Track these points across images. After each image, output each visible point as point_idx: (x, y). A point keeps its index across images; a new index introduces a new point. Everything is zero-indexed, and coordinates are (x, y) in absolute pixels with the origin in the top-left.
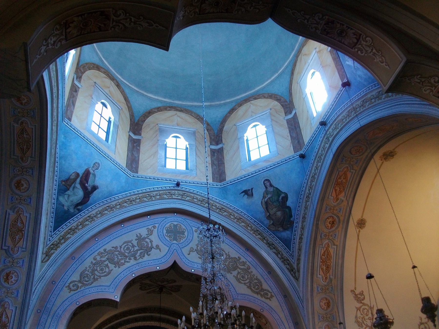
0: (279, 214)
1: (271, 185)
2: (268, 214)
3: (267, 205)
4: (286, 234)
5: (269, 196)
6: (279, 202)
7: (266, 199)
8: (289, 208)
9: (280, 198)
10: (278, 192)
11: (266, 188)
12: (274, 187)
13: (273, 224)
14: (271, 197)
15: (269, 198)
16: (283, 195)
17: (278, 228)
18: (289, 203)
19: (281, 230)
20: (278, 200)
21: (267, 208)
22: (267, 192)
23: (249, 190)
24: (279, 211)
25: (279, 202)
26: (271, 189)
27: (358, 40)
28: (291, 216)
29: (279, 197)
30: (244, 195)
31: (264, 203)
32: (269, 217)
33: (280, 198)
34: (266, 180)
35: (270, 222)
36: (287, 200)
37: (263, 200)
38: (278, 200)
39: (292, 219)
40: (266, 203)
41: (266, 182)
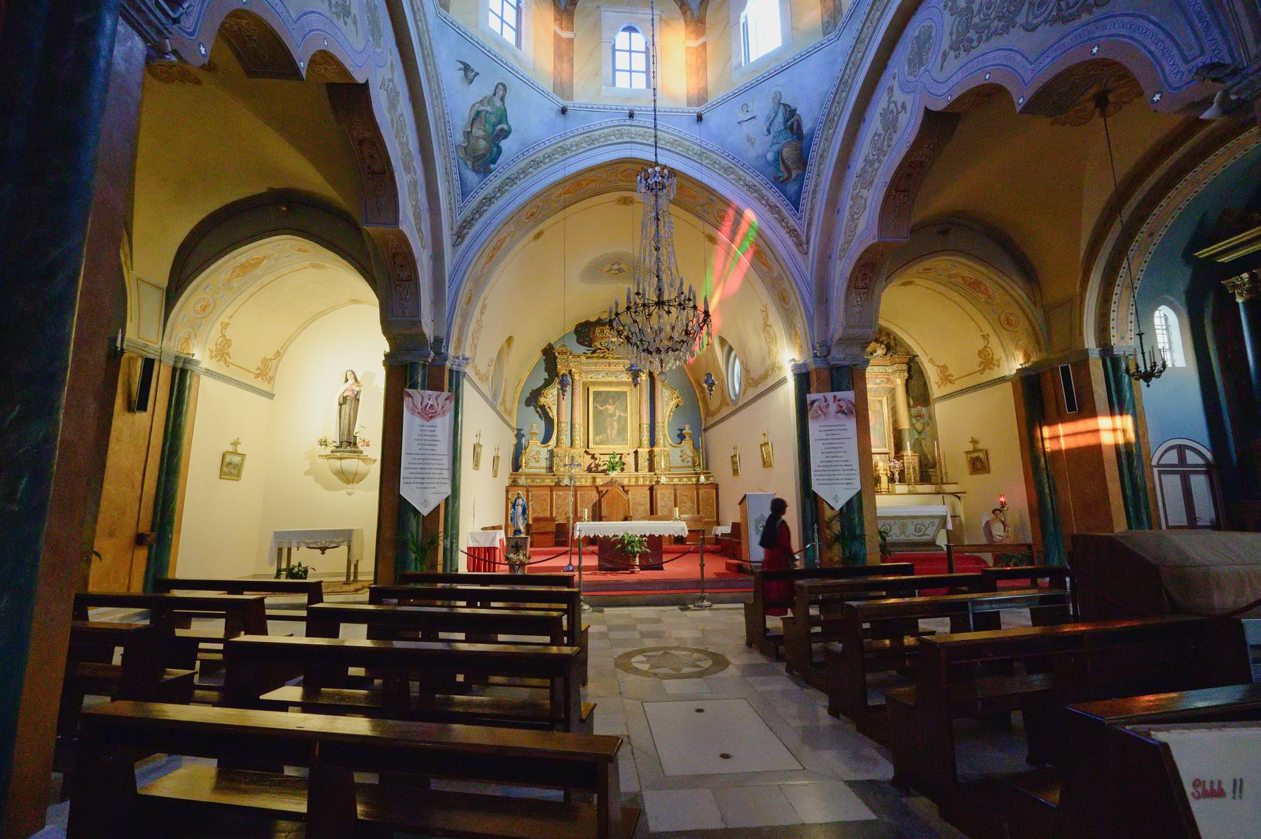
0: (482, 143)
1: (502, 99)
2: (469, 130)
3: (477, 116)
4: (471, 177)
5: (489, 109)
6: (494, 130)
7: (481, 108)
8: (500, 151)
9: (499, 127)
10: (503, 117)
11: (495, 94)
12: (503, 105)
13: (465, 148)
14: (490, 113)
15: (487, 112)
16: (505, 127)
17: (468, 160)
18: (504, 144)
19: (470, 167)
20: (494, 126)
21: (474, 119)
22: (489, 101)
23: (473, 70)
24: (485, 139)
25: (494, 130)
26: (498, 104)
27: (904, 191)
28: (494, 161)
29: (499, 124)
30: (461, 69)
31: (476, 109)
32: (468, 135)
33: (499, 127)
34: (504, 85)
35: (464, 142)
36: (505, 138)
37: (478, 105)
38: (494, 126)
39: (492, 166)
40: (478, 113)
41: (500, 87)
